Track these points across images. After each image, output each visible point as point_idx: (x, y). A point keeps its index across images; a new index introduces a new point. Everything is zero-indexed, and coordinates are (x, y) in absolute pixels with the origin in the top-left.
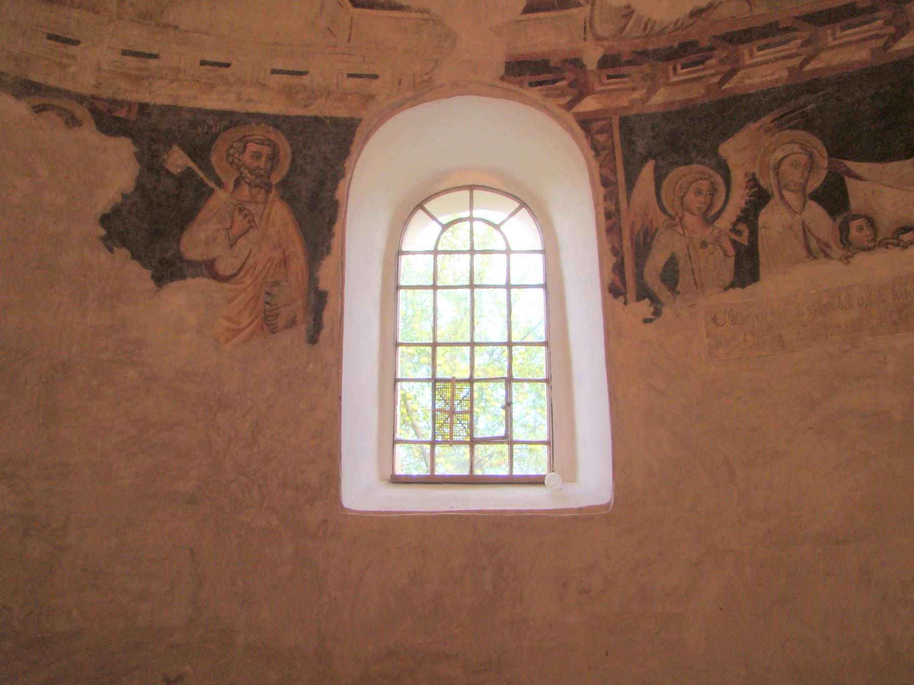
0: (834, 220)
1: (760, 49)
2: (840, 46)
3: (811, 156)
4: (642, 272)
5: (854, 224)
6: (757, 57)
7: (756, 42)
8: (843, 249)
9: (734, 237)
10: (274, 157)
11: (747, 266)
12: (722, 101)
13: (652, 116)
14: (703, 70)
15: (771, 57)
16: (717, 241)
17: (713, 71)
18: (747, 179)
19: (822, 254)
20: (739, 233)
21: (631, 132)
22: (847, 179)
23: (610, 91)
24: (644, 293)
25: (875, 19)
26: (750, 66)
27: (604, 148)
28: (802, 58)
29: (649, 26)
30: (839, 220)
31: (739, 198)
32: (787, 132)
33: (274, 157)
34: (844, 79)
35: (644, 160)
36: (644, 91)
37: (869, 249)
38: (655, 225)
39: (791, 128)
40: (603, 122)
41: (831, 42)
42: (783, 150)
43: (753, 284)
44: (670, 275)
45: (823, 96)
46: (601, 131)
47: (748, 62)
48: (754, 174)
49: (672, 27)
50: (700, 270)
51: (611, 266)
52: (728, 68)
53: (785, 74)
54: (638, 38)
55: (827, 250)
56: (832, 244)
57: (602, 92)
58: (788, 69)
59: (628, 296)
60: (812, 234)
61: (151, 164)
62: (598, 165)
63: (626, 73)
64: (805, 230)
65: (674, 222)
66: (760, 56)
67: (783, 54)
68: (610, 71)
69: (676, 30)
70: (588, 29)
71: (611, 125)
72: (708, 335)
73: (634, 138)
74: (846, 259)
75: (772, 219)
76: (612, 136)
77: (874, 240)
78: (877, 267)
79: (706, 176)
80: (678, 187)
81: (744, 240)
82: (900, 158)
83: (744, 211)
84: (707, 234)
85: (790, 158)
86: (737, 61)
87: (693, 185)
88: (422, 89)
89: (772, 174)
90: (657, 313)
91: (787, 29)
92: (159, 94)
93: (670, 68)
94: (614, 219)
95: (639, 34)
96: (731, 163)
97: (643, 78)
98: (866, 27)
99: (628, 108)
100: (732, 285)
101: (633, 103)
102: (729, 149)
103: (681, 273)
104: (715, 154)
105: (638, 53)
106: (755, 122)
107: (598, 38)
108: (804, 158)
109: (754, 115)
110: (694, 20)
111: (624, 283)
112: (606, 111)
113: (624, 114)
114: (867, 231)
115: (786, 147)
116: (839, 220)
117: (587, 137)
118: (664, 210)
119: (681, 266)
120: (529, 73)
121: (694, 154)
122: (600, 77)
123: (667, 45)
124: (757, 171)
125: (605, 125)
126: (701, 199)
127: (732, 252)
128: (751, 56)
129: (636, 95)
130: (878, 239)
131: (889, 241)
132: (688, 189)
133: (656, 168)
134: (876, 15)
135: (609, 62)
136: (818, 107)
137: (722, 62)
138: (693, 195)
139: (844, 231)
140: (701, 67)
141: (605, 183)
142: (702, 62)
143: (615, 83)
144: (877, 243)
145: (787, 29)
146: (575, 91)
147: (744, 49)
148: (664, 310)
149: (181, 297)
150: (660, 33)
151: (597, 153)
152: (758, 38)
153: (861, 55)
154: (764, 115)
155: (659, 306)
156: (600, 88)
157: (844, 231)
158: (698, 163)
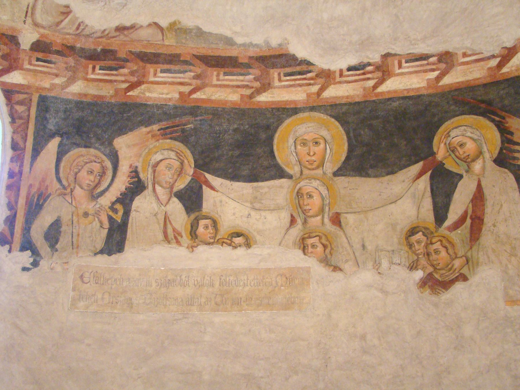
0: (189, 217)
1: (162, 71)
2: (220, 86)
3: (182, 163)
4: (30, 228)
5: (202, 223)
6: (159, 77)
7: (161, 65)
8: (191, 239)
9: (111, 213)
11: (116, 239)
12: (125, 104)
13: (67, 102)
14: (116, 75)
15: (170, 80)
16: (97, 214)
17: (123, 79)
18: (131, 170)
19: (175, 241)
20: (116, 211)
21: (47, 110)
22: (204, 187)
23: (35, 71)
24: (28, 245)
25: (249, 74)
26: (153, 83)
27: (21, 118)
28: (192, 87)
29: (82, 27)
30: (193, 216)
31: (121, 184)
32: (168, 141)
34: (217, 112)
35: (52, 136)
36: (66, 79)
37: (209, 244)
38: (49, 191)
39: (171, 138)
40: (25, 96)
41: (215, 82)
42: (163, 154)
43: (118, 254)
44: (53, 235)
45: (201, 120)
46: (21, 103)
47: (152, 79)
48: (137, 167)
49: (99, 34)
50: (78, 235)
51: (4, 217)
52: (136, 79)
53: (177, 96)
54: (69, 34)
55: (179, 238)
56: (183, 234)
57: (29, 70)
58: (181, 93)
59: (13, 245)
60: (171, 224)
62: (12, 130)
63: (54, 60)
64: (166, 219)
65: (66, 191)
66: (162, 77)
67: (179, 80)
68: (40, 55)
69: (101, 37)
70: (29, 14)
71: (31, 100)
72: (74, 290)
73: (48, 116)
74: (192, 248)
75: (143, 205)
76: (29, 110)
77: (214, 238)
78: (213, 259)
79: (99, 161)
80: (75, 163)
81: (118, 217)
82: (245, 181)
83: (123, 194)
84: (91, 207)
85: (167, 161)
86: (144, 76)
87: (88, 165)
89: (150, 170)
90: (35, 264)
91: (186, 62)
93: (91, 66)
94: (15, 178)
95: (71, 31)
96: (122, 154)
97: (66, 68)
98: (241, 78)
99: (49, 90)
100: (101, 252)
101: (53, 86)
102: (123, 144)
103: (62, 234)
104: (111, 143)
105: (68, 47)
106: (146, 127)
107: (36, 25)
108: (176, 164)
109: (147, 122)
110: (118, 34)
111: (12, 234)
112: (29, 87)
113: (43, 94)
114: (211, 230)
115: (166, 152)
116: (193, 216)
117: (7, 105)
118: (59, 180)
119: (63, 229)
121: (93, 140)
122: (30, 57)
123: (93, 47)
124: (140, 165)
125: (25, 99)
126: (92, 178)
127: (106, 225)
128: (155, 75)
129: (57, 81)
130: (217, 238)
131: (225, 240)
132: (82, 167)
133: (60, 145)
134: (251, 71)
135: (41, 47)
136: (195, 128)
137: (132, 73)
138: (85, 173)
139: (194, 226)
140: (114, 72)
141: (15, 146)
142: (116, 69)
143: (41, 67)
144: (216, 241)
145: (186, 62)
146: (6, 64)
147: (151, 69)
148: (43, 263)
150: (88, 36)
151: (13, 121)
152: (163, 64)
153: (234, 97)
154: (154, 124)
155: (38, 259)
156: (28, 67)
157: (194, 226)
158: (95, 148)
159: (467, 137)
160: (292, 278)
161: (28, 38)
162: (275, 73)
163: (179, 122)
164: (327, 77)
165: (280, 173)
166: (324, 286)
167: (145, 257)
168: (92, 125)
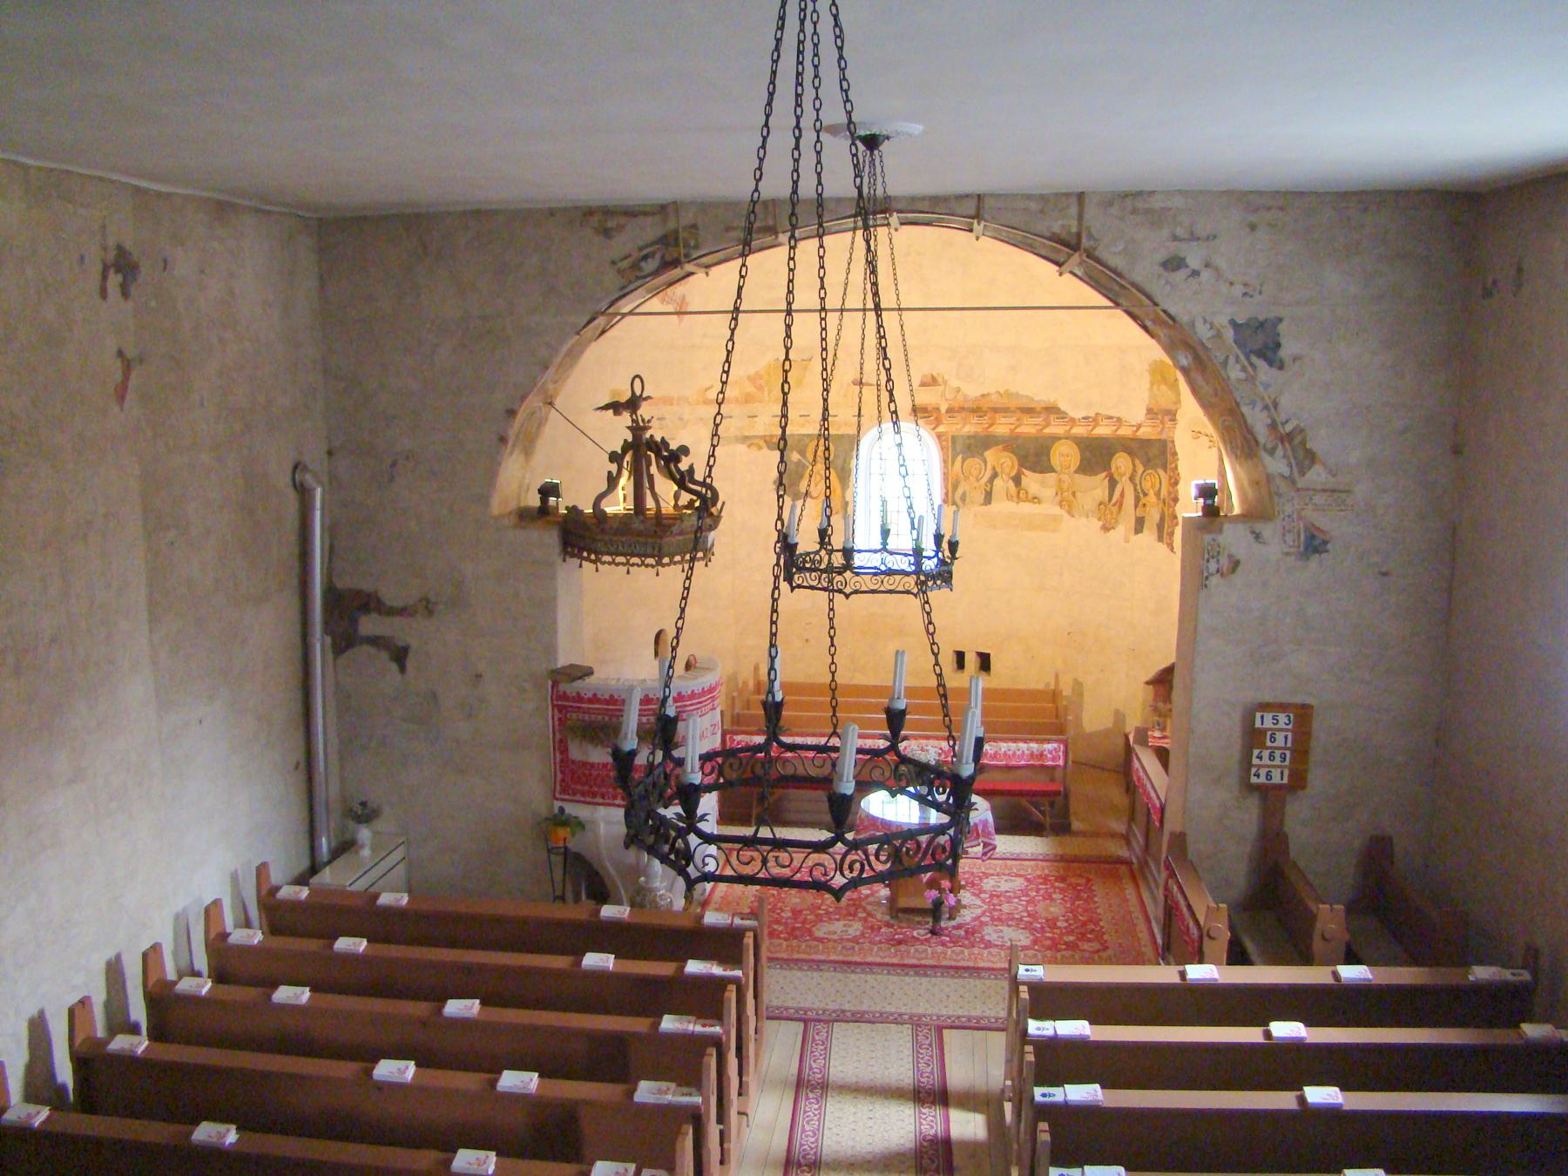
11: (988, 498)
24: (954, 503)
34: (1028, 438)
44: (963, 498)
65: (967, 478)
66: (1003, 420)
75: (997, 482)
78: (1026, 508)
102: (988, 454)
135: (950, 410)
141: (945, 461)
153: (1033, 430)
159: (1121, 462)
160: (1055, 518)
161: (943, 409)
162: (1052, 417)
163: (1011, 444)
164: (1073, 420)
165: (1053, 471)
166: (1068, 523)
167: (1001, 506)
168: (976, 446)
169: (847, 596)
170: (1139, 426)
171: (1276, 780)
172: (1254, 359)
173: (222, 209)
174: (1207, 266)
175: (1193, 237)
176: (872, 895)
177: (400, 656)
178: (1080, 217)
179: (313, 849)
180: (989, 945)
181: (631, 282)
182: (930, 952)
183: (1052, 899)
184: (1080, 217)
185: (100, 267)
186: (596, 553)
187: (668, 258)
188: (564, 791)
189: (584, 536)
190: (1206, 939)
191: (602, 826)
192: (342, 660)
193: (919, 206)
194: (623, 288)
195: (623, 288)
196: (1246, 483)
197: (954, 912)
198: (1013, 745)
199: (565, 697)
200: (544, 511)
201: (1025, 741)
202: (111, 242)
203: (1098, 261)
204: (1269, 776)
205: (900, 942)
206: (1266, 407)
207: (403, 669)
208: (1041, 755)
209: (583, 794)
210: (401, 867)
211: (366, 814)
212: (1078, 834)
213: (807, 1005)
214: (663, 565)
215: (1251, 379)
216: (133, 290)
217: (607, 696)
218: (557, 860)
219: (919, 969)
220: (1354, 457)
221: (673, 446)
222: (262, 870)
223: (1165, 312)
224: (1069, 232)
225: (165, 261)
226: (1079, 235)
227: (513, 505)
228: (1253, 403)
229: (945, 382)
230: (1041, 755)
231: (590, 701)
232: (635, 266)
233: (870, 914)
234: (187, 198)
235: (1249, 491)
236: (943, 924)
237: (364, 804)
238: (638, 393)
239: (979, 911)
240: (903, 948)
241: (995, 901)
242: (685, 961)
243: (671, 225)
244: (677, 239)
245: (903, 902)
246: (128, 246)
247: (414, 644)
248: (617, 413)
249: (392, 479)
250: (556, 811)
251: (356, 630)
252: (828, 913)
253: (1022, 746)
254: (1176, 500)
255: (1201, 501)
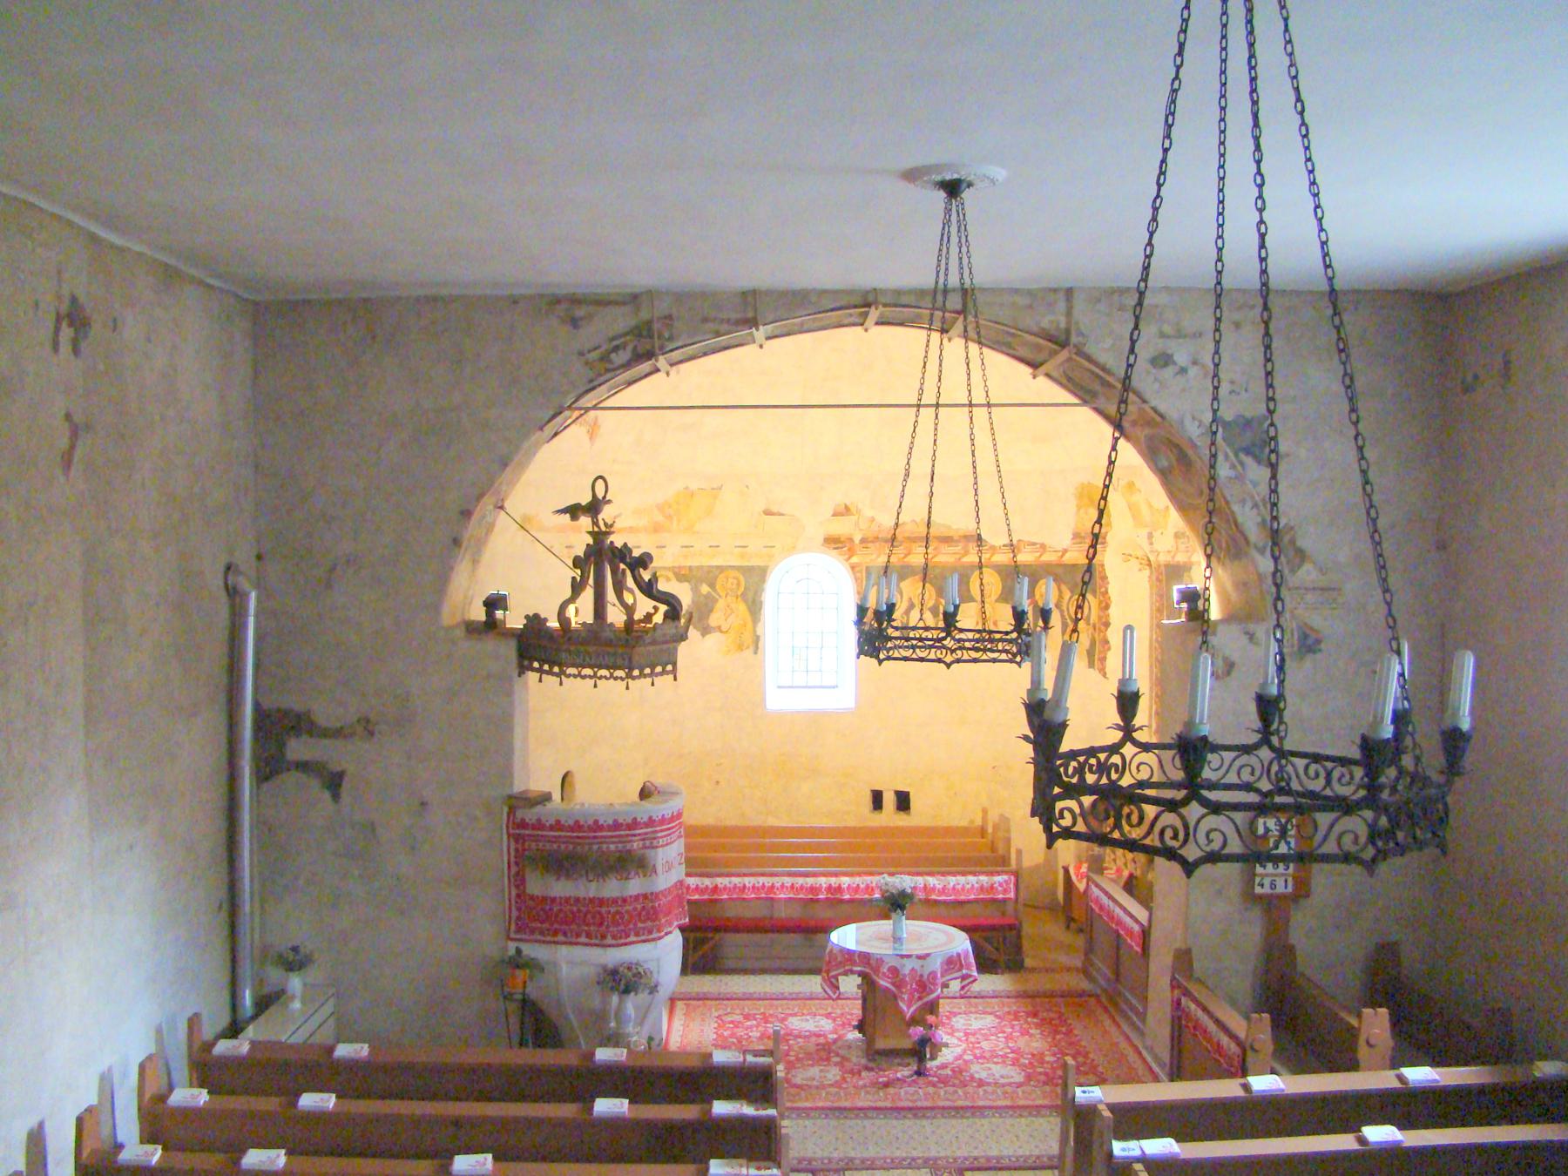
10: (739, 584)
33: (739, 584)
61: (695, 591)
88: (793, 549)
92: (694, 562)
120: (833, 542)
135: (863, 541)
149: (712, 638)
161: (857, 541)
169: (948, 666)
170: (1065, 551)
171: (1280, 889)
172: (1242, 456)
173: (169, 276)
174: (1195, 363)
175: (1179, 334)
176: (840, 1037)
177: (334, 782)
178: (1069, 314)
179: (234, 1007)
180: (981, 1083)
181: (600, 375)
182: (907, 1095)
183: (1031, 1036)
184: (1069, 314)
185: (53, 316)
186: (560, 665)
187: (641, 350)
188: (519, 930)
189: (541, 647)
190: (1249, 1053)
191: (564, 968)
192: (265, 786)
193: (904, 300)
194: (591, 381)
195: (591, 381)
196: (1229, 586)
197: (937, 1048)
198: (962, 879)
199: (523, 825)
200: (491, 625)
201: (974, 874)
202: (66, 291)
203: (1089, 359)
204: (1273, 885)
205: (886, 1085)
206: (1255, 506)
207: (336, 796)
208: (992, 887)
209: (542, 933)
210: (331, 1021)
211: (295, 961)
212: (1033, 970)
213: (809, 1154)
214: (634, 678)
215: (1240, 478)
216: (83, 345)
217: (571, 822)
218: (513, 1007)
219: (916, 1112)
220: (1343, 556)
221: (636, 553)
222: (194, 1022)
223: (1155, 410)
224: (1058, 328)
225: (115, 320)
226: (1068, 331)
227: (458, 618)
228: (1243, 502)
229: (858, 511)
230: (992, 887)
231: (552, 828)
232: (605, 358)
233: (844, 1058)
234: (140, 255)
235: (1234, 596)
236: (929, 1064)
237: (295, 949)
238: (600, 495)
239: (959, 1050)
240: (891, 1090)
241: (972, 1039)
242: (710, 1103)
243: (645, 315)
244: (650, 329)
245: (881, 1044)
246: (82, 298)
247: (351, 769)
248: (574, 517)
249: (329, 585)
250: (512, 952)
251: (283, 754)
252: (798, 1059)
253: (972, 879)
254: (1107, 625)
255: (1184, 605)
